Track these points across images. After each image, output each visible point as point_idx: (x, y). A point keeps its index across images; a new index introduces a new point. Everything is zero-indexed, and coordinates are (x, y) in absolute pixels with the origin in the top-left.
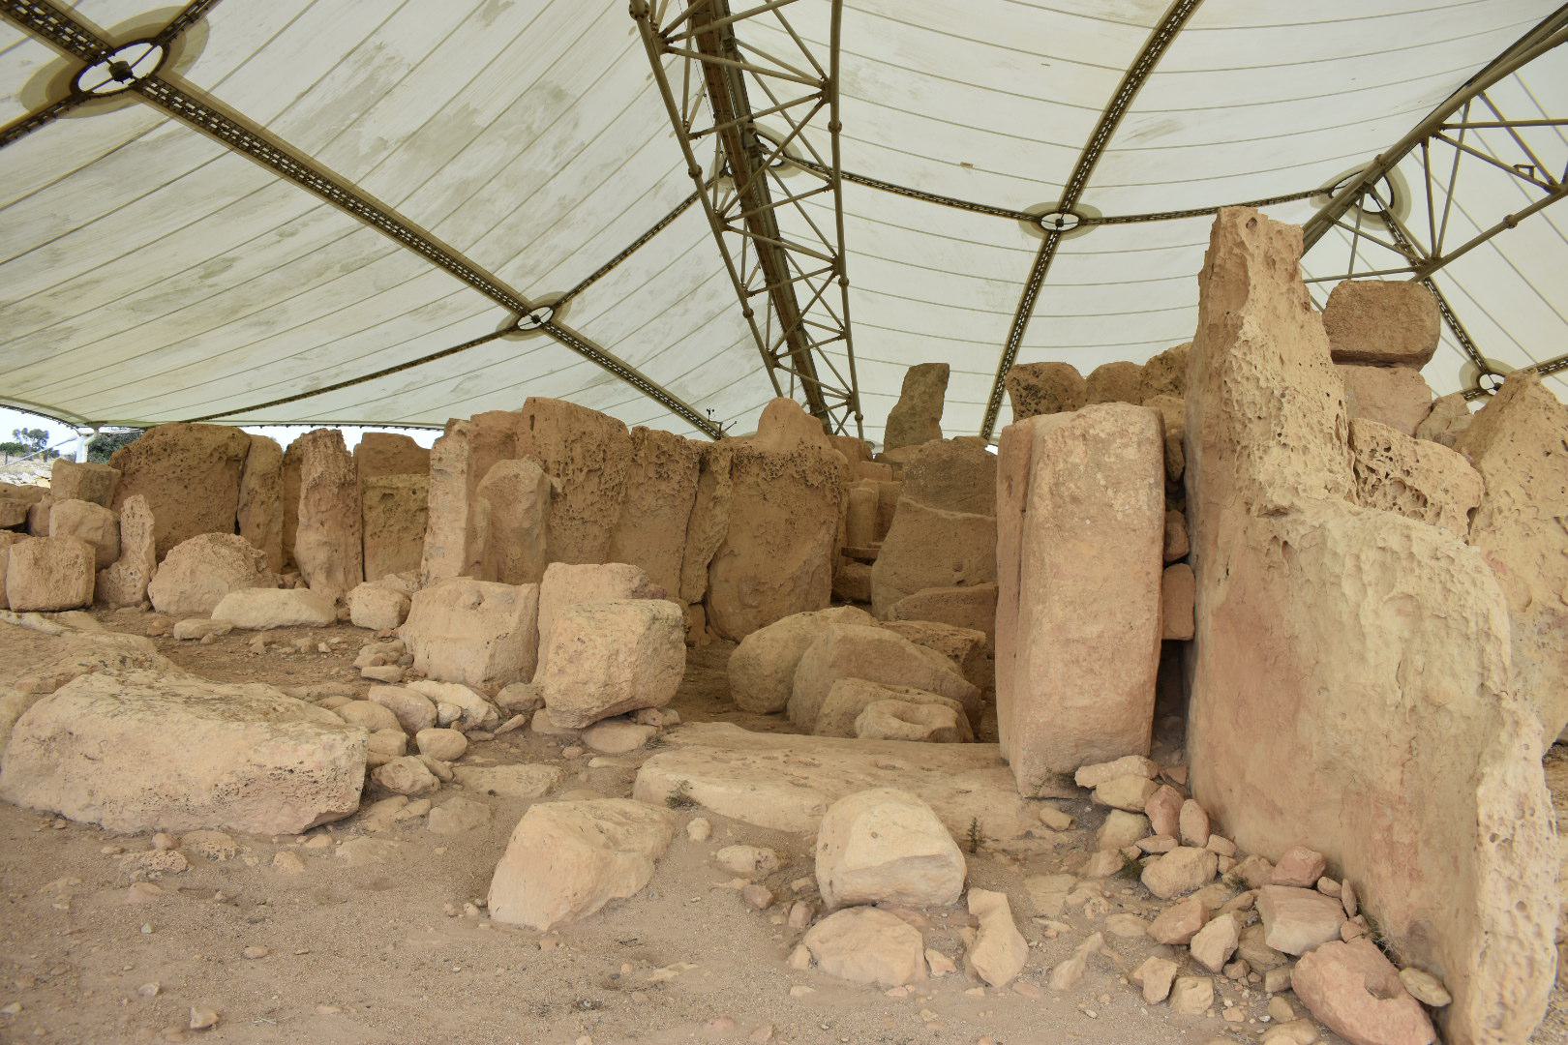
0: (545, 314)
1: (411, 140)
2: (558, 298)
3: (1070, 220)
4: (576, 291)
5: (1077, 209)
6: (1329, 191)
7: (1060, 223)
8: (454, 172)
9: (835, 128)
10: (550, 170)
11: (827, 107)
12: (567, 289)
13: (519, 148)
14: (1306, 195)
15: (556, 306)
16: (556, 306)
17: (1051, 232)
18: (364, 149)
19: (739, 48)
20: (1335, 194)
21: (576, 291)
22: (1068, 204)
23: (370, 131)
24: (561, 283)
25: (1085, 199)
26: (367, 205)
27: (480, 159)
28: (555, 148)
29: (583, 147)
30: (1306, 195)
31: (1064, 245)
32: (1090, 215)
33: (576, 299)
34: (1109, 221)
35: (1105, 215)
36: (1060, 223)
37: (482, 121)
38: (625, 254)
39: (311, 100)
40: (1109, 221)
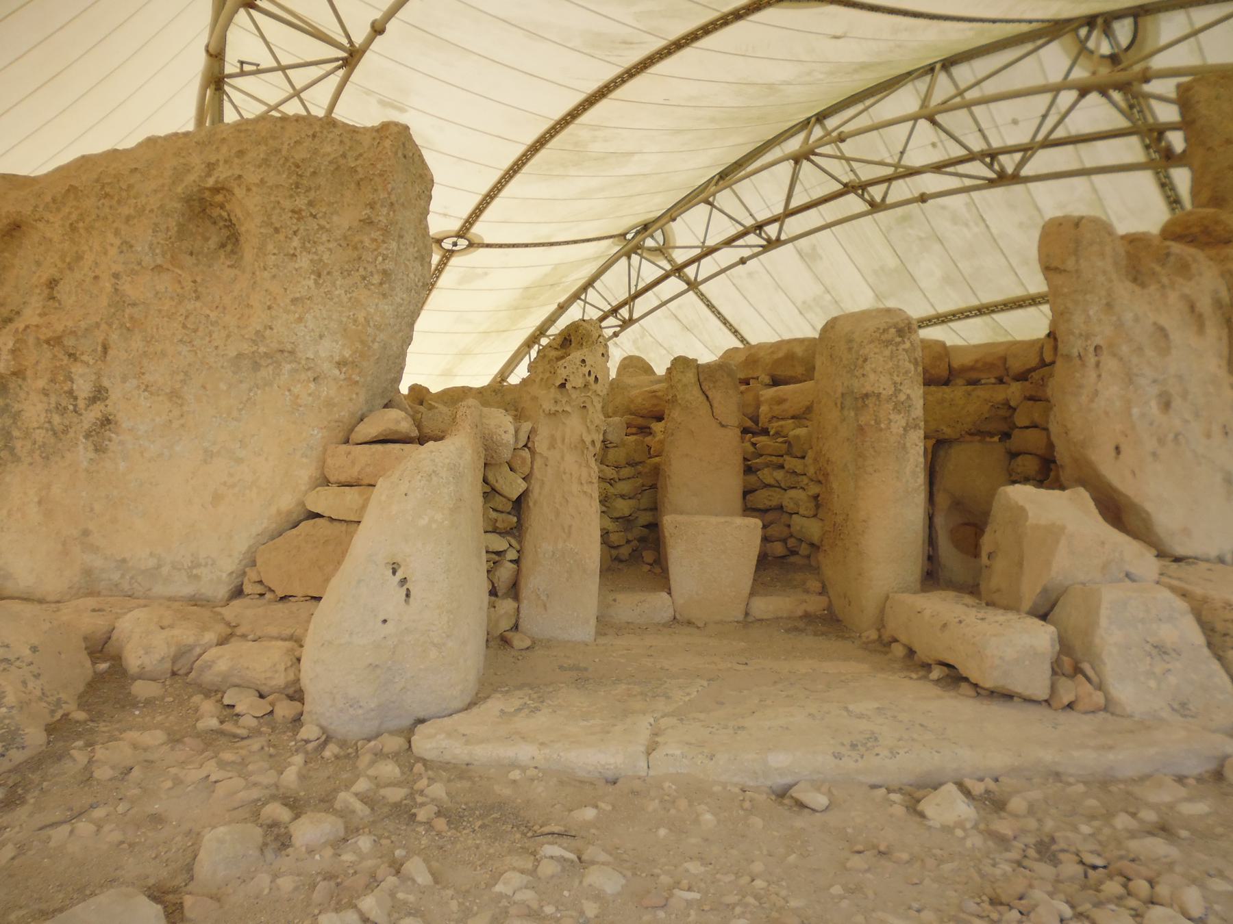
3: (463, 243)
5: (468, 236)
6: (624, 235)
7: (455, 244)
14: (611, 237)
17: (448, 251)
19: (226, 88)
20: (629, 236)
22: (461, 234)
25: (480, 230)
30: (611, 237)
31: (454, 261)
32: (476, 241)
34: (488, 246)
35: (487, 241)
36: (455, 244)
40: (488, 246)
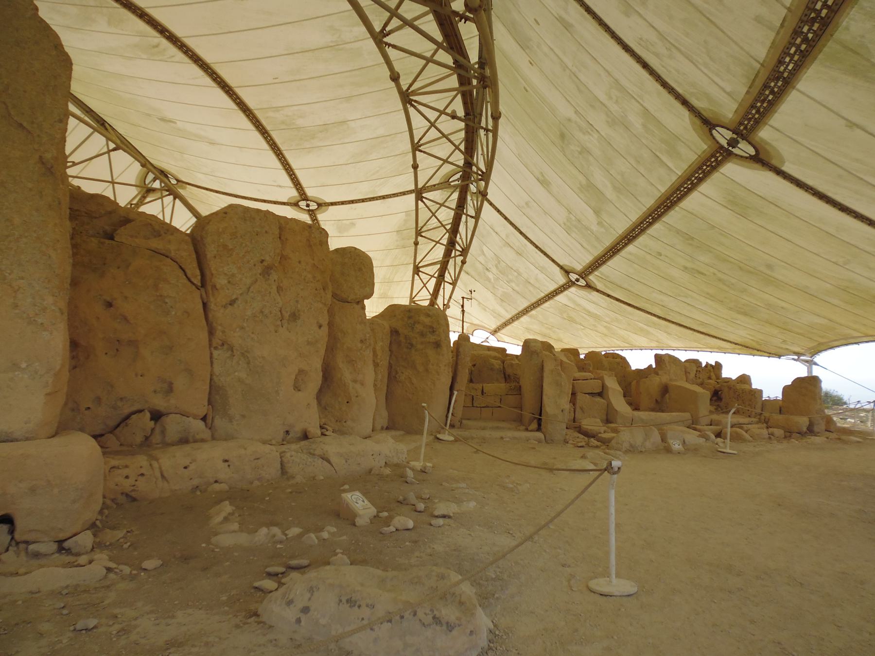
0: (723, 136)
1: (597, 212)
2: (698, 122)
4: (685, 103)
8: (610, 193)
9: (395, 78)
10: (596, 136)
11: (405, 88)
12: (685, 113)
13: (591, 158)
15: (708, 124)
16: (708, 124)
18: (603, 230)
21: (685, 103)
23: (594, 228)
24: (679, 121)
26: (631, 232)
27: (599, 179)
28: (584, 133)
29: (576, 112)
33: (694, 102)
37: (584, 181)
38: (626, 48)
39: (585, 245)
